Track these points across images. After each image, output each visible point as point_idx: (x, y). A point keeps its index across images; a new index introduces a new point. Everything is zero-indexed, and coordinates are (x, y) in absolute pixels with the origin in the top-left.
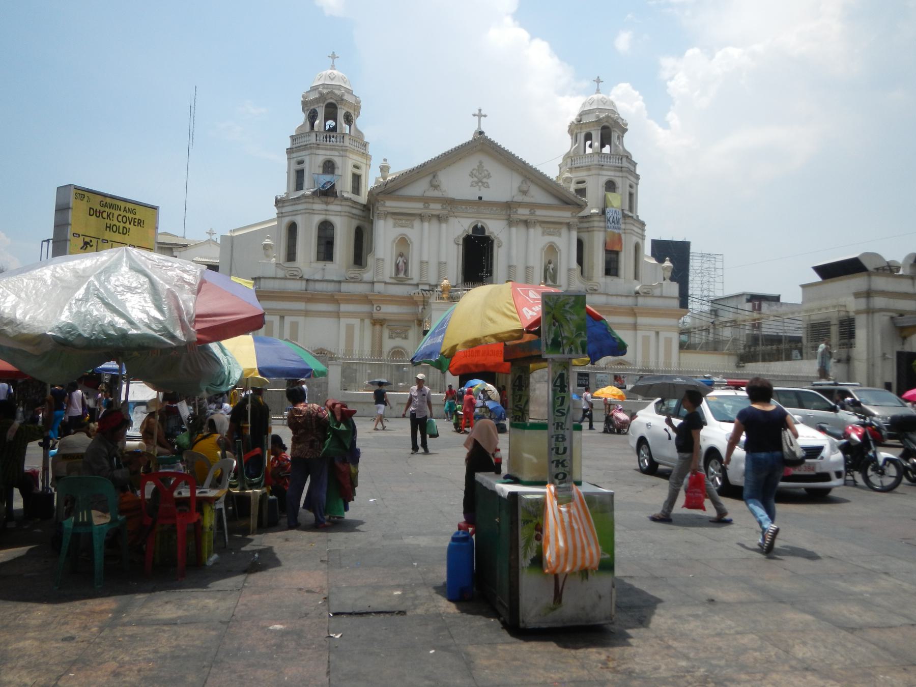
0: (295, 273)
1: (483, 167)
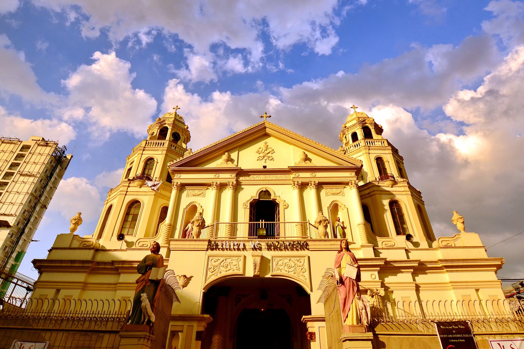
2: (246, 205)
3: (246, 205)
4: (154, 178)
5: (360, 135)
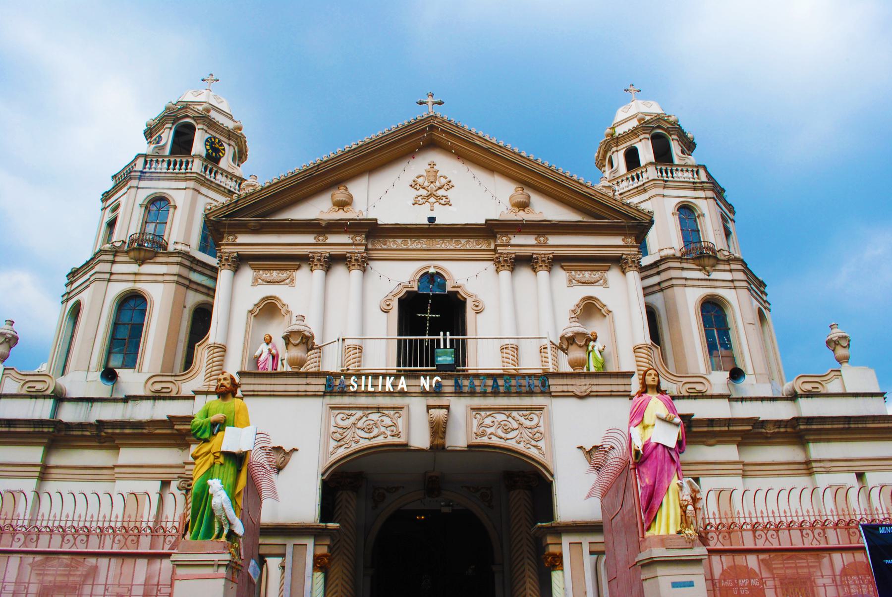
0: (39, 386)
1: (437, 172)
2: (388, 305)
3: (388, 305)
4: (171, 243)
5: (646, 153)
